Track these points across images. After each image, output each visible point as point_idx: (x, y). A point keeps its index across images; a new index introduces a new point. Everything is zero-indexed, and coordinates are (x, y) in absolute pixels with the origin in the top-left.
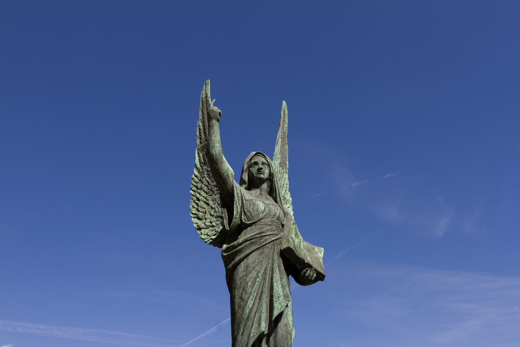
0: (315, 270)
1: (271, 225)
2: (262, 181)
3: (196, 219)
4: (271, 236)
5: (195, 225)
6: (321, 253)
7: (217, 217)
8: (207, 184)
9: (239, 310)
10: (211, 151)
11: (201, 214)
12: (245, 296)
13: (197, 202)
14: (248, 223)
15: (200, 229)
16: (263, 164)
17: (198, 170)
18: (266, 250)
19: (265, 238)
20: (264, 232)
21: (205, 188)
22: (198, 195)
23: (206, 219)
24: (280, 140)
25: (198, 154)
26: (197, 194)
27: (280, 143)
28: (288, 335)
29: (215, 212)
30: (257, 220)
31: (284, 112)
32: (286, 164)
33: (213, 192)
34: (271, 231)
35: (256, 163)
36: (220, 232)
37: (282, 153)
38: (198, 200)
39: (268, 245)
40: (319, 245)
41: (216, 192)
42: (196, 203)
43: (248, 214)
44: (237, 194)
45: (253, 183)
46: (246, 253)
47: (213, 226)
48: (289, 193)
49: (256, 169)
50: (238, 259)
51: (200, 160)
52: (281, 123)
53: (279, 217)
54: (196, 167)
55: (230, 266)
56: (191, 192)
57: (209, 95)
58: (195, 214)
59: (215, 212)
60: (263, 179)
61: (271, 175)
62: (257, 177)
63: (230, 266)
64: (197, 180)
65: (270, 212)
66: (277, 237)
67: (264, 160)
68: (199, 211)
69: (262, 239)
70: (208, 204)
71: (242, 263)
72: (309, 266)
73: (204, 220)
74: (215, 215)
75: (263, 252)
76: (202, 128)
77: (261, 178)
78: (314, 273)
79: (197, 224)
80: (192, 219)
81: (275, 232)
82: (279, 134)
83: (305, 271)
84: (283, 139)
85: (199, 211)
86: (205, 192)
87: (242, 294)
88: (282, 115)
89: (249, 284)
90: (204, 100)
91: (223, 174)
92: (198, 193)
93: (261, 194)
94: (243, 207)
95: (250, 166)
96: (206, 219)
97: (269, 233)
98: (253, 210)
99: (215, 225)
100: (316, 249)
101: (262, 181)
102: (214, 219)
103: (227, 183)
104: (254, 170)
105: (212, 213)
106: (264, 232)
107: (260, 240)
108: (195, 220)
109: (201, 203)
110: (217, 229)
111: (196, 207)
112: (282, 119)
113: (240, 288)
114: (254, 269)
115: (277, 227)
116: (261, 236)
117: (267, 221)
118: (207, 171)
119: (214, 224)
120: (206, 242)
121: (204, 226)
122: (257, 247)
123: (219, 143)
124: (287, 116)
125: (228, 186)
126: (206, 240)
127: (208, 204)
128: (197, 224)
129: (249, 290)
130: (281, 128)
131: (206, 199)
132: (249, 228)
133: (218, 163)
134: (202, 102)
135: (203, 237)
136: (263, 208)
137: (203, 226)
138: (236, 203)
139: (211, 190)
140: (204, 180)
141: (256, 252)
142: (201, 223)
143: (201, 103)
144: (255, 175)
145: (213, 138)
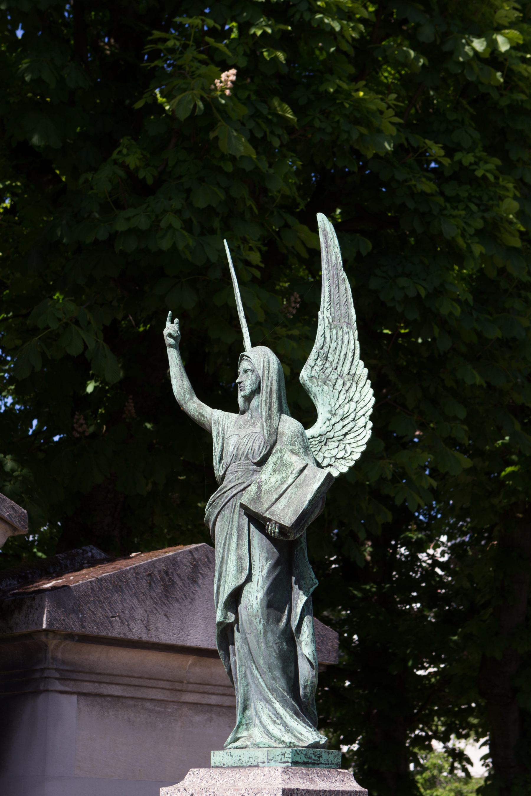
0: (276, 523)
4: (233, 489)
18: (227, 512)
19: (226, 495)
28: (253, 618)
31: (324, 231)
39: (228, 504)
44: (218, 433)
48: (362, 363)
53: (247, 455)
66: (242, 487)
69: (222, 497)
72: (270, 520)
75: (224, 516)
78: (275, 527)
81: (240, 481)
93: (252, 418)
94: (222, 451)
107: (221, 499)
122: (218, 510)
123: (175, 378)
125: (207, 426)
141: (219, 517)
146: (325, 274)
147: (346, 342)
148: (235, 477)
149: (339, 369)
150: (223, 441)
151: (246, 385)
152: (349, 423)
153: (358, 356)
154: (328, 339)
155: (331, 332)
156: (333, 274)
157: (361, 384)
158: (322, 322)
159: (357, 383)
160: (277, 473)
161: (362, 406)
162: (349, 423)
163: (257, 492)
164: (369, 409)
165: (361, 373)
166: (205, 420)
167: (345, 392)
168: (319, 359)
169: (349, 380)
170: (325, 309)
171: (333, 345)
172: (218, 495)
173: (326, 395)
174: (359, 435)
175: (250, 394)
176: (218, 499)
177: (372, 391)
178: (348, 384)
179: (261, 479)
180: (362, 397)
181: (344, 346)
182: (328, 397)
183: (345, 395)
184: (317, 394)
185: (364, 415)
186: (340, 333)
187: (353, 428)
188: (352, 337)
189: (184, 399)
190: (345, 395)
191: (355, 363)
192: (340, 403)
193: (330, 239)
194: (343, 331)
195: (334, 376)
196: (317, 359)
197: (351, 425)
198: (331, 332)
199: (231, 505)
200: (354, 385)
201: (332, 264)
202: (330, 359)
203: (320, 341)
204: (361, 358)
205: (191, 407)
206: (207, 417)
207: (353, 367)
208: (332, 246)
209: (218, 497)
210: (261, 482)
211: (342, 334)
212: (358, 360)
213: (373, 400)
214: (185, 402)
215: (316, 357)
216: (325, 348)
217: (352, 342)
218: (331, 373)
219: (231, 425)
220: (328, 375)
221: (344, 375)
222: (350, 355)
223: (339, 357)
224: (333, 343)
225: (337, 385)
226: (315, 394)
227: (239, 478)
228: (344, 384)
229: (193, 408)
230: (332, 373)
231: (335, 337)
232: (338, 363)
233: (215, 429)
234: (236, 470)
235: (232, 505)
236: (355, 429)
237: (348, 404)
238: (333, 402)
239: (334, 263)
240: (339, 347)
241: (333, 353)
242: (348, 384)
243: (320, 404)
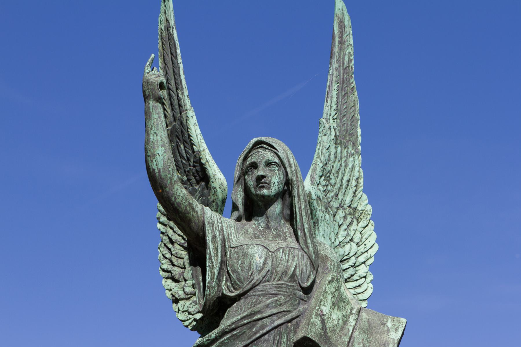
1: (276, 295)
2: (269, 201)
3: (169, 281)
4: (275, 318)
5: (168, 294)
6: (396, 330)
11: (176, 271)
13: (170, 246)
14: (232, 295)
15: (176, 301)
16: (269, 164)
19: (260, 323)
20: (259, 312)
22: (170, 232)
23: (186, 281)
24: (335, 87)
26: (169, 229)
27: (335, 93)
30: (249, 287)
32: (353, 134)
34: (275, 307)
35: (254, 166)
37: (341, 113)
38: (172, 242)
39: (266, 336)
40: (396, 314)
43: (234, 276)
44: (214, 237)
45: (253, 207)
48: (365, 197)
49: (254, 178)
52: (336, 49)
56: (159, 226)
57: (172, 23)
60: (269, 196)
61: (288, 183)
65: (275, 266)
66: (289, 317)
67: (270, 156)
69: (254, 326)
73: (183, 283)
77: (263, 196)
79: (171, 290)
80: (164, 281)
81: (284, 308)
82: (333, 73)
84: (343, 82)
85: (173, 265)
88: (336, 31)
90: (165, 34)
91: (179, 204)
93: (268, 227)
94: (223, 263)
95: (244, 173)
96: (186, 281)
97: (268, 313)
98: (242, 267)
100: (389, 324)
101: (269, 201)
103: (190, 221)
104: (251, 181)
106: (259, 312)
107: (251, 328)
108: (169, 283)
111: (168, 256)
112: (337, 40)
115: (291, 296)
116: (252, 320)
117: (269, 286)
120: (187, 326)
123: (162, 146)
124: (349, 30)
125: (193, 225)
126: (186, 323)
128: (171, 290)
130: (334, 61)
132: (235, 304)
133: (166, 186)
134: (162, 39)
135: (181, 316)
136: (262, 261)
137: (181, 294)
138: (210, 258)
142: (177, 289)
143: (160, 41)
144: (253, 190)
145: (151, 137)
146: (335, 74)
147: (350, 166)
148: (276, 301)
149: (340, 196)
150: (224, 252)
151: (273, 182)
152: (349, 268)
153: (362, 188)
154: (332, 156)
155: (336, 148)
156: (343, 78)
157: (362, 224)
158: (328, 133)
159: (357, 220)
160: (336, 307)
161: (363, 250)
162: (349, 268)
163: (322, 328)
164: (371, 257)
165: (363, 208)
166: (195, 215)
167: (346, 227)
168: (323, 178)
169: (350, 214)
170: (331, 117)
171: (337, 165)
172: (246, 321)
173: (327, 225)
174: (359, 286)
175: (275, 195)
176: (245, 327)
177: (374, 236)
178: (349, 219)
179: (322, 311)
180: (364, 240)
181: (347, 170)
182: (329, 228)
183: (346, 232)
184: (320, 221)
185: (364, 263)
186: (345, 153)
187: (353, 275)
188: (357, 162)
189: (171, 178)
190: (346, 232)
191: (359, 194)
192: (341, 239)
193: (346, 35)
194: (347, 152)
195: (335, 205)
196: (321, 177)
197: (351, 271)
198: (336, 148)
199: (272, 338)
200: (355, 220)
201: (343, 64)
202: (333, 181)
203: (326, 155)
204: (364, 191)
205: (180, 192)
206: (197, 212)
207: (356, 199)
208: (346, 44)
209: (245, 325)
210: (323, 315)
211: (346, 155)
212: (361, 193)
213: (376, 247)
214: (171, 183)
215: (321, 174)
216: (328, 165)
217: (357, 169)
218: (332, 198)
219: (233, 231)
220: (329, 200)
221: (345, 206)
222: (354, 183)
223: (342, 183)
224: (337, 162)
225: (337, 217)
226: (318, 220)
227: (281, 305)
228: (345, 218)
229: (182, 195)
230: (333, 200)
231: (340, 155)
232: (339, 189)
233: (210, 232)
234: (274, 292)
235: (274, 340)
236: (355, 277)
237: (349, 244)
238: (333, 236)
239: (346, 65)
240: (342, 169)
241: (336, 175)
242: (349, 219)
243: (321, 234)
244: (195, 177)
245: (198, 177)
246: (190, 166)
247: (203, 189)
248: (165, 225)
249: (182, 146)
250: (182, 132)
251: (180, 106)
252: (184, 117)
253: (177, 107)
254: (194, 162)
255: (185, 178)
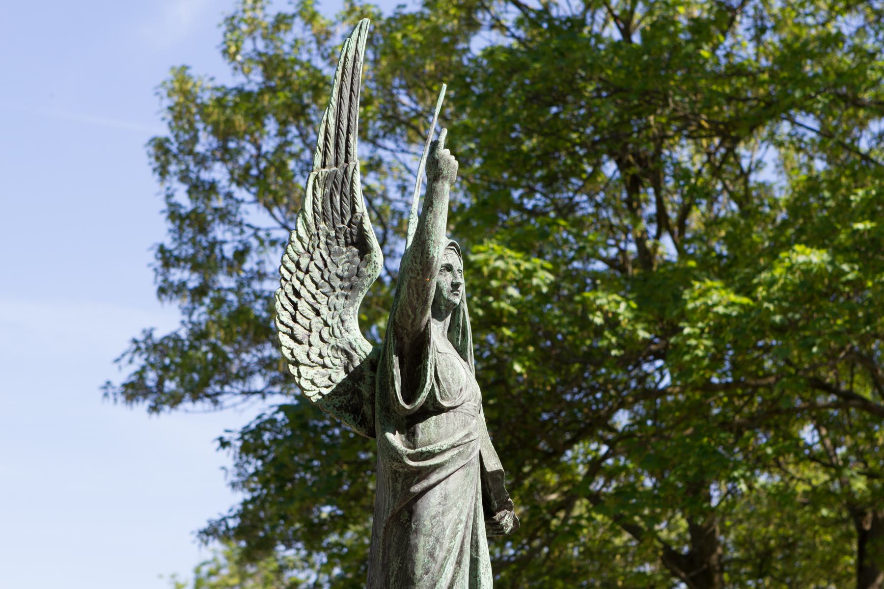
3: (287, 337)
7: (336, 348)
8: (321, 265)
9: (425, 577)
10: (431, 249)
11: (300, 332)
12: (440, 554)
17: (308, 225)
21: (316, 274)
25: (314, 188)
26: (294, 279)
29: (332, 334)
33: (333, 289)
36: (339, 385)
38: (297, 294)
41: (338, 291)
42: (290, 299)
46: (450, 471)
47: (324, 366)
49: (449, 283)
50: (434, 478)
51: (314, 203)
54: (305, 219)
55: (416, 488)
56: (283, 270)
58: (287, 326)
59: (332, 334)
62: (449, 300)
63: (416, 488)
64: (302, 250)
68: (294, 319)
70: (318, 313)
71: (437, 488)
73: (307, 347)
74: (332, 341)
76: (332, 130)
83: (501, 513)
85: (294, 319)
86: (313, 281)
87: (434, 548)
89: (447, 532)
92: (298, 278)
96: (310, 345)
99: (330, 365)
102: (326, 351)
105: (326, 336)
109: (302, 305)
110: (334, 377)
111: (291, 309)
113: (430, 536)
114: (455, 504)
118: (328, 236)
119: (327, 361)
121: (307, 361)
127: (318, 313)
129: (446, 545)
131: (314, 297)
139: (329, 282)
140: (316, 255)
144: (445, 293)
244: (346, 238)
245: (349, 240)
246: (343, 223)
247: (354, 256)
248: (291, 273)
249: (338, 197)
250: (343, 182)
251: (347, 152)
252: (352, 168)
253: (343, 151)
254: (350, 221)
255: (333, 233)
